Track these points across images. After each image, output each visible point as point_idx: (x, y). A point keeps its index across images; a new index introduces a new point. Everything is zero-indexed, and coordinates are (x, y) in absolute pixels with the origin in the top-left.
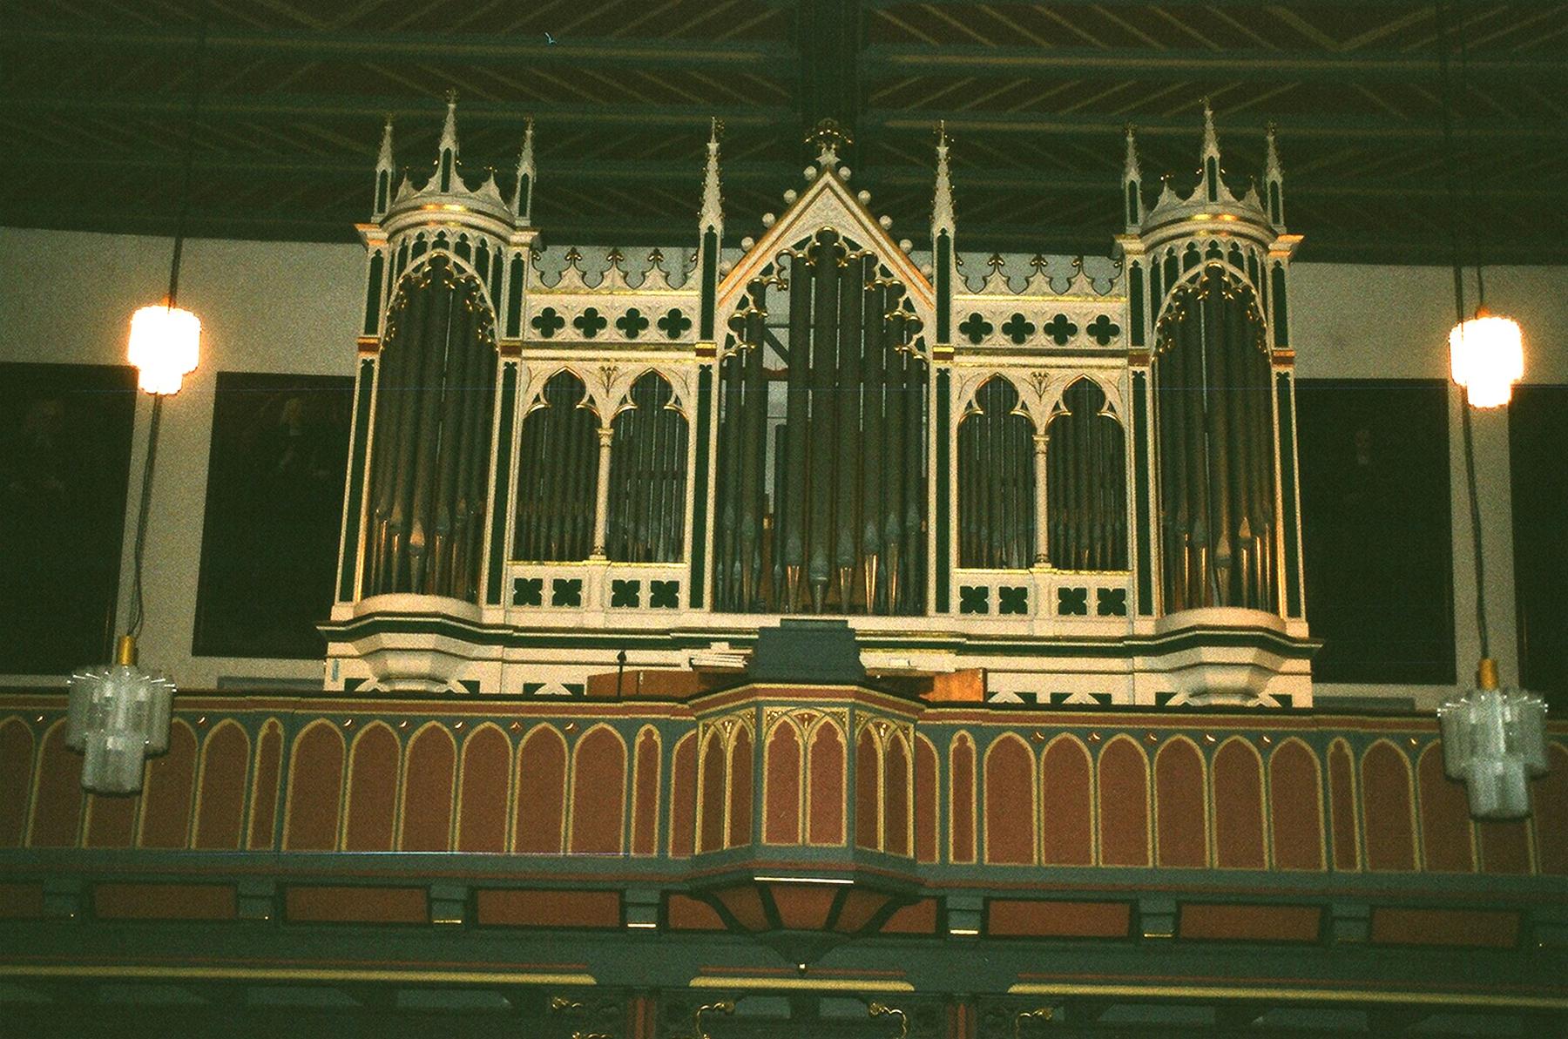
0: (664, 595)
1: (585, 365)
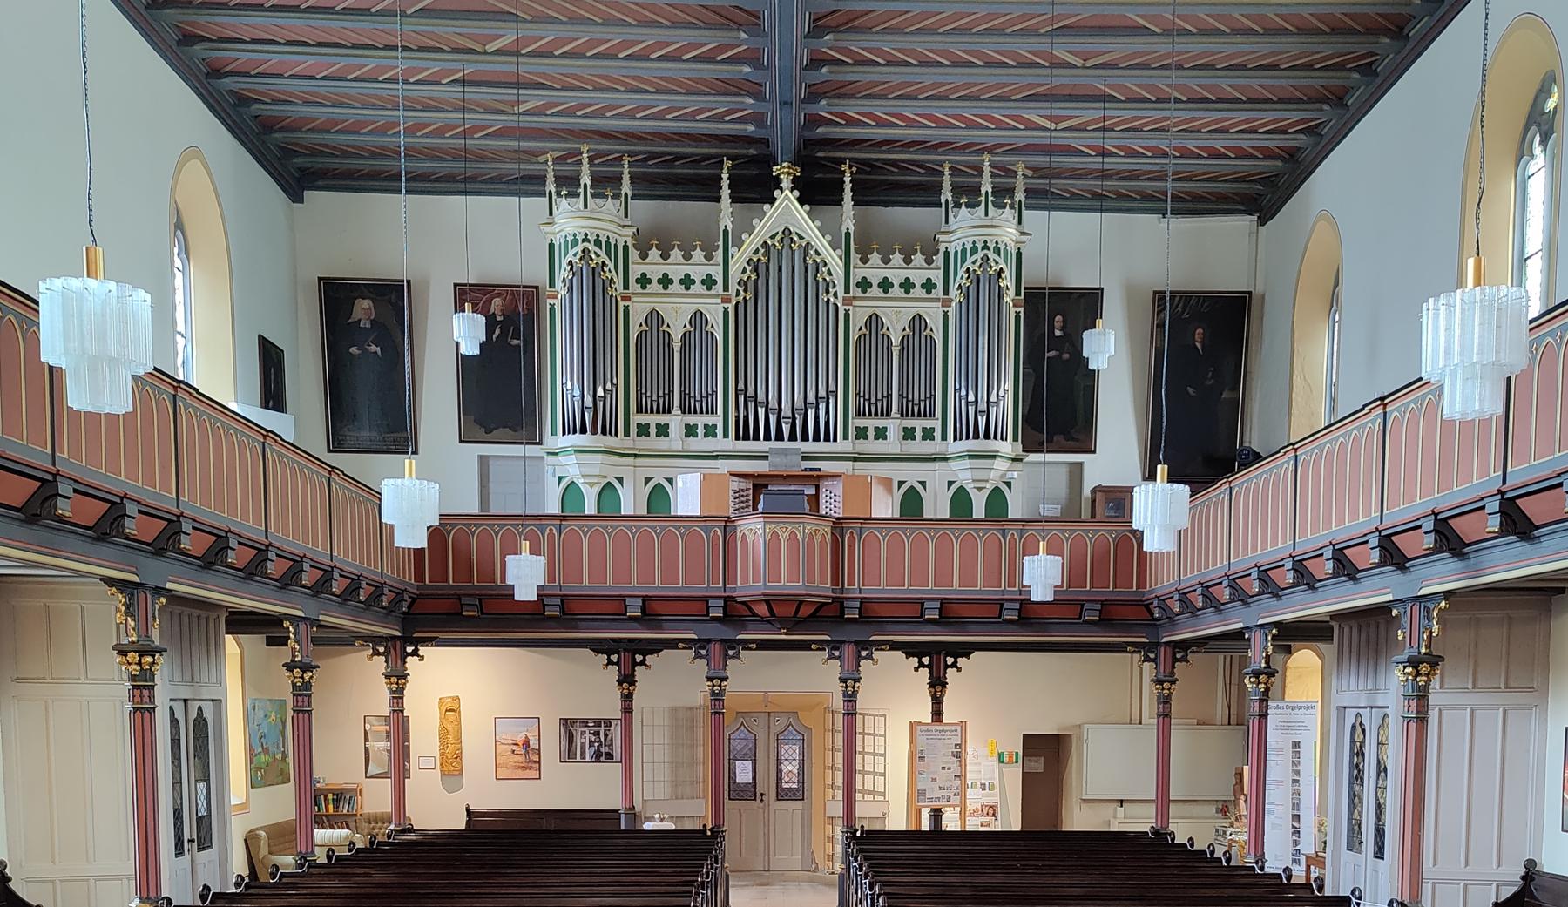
0: (710, 431)
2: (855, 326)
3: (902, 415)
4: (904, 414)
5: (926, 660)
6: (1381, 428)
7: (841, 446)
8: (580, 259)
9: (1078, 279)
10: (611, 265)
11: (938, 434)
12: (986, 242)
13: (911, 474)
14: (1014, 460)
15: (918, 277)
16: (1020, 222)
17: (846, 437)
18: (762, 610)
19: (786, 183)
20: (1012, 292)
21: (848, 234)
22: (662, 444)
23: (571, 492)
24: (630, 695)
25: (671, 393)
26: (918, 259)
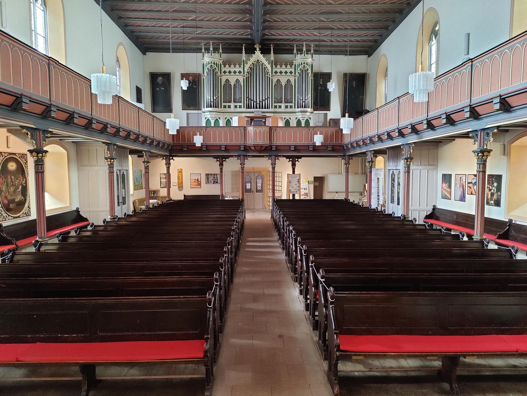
0: (240, 107)
2: (274, 83)
3: (285, 103)
4: (285, 102)
5: (291, 159)
6: (470, 70)
7: (271, 110)
8: (210, 67)
9: (326, 70)
10: (217, 69)
11: (293, 107)
12: (304, 62)
13: (287, 116)
14: (311, 113)
15: (288, 70)
16: (312, 57)
17: (272, 108)
18: (253, 148)
19: (258, 49)
20: (310, 74)
21: (272, 61)
23: (208, 121)
24: (222, 168)
25: (231, 98)
26: (289, 66)
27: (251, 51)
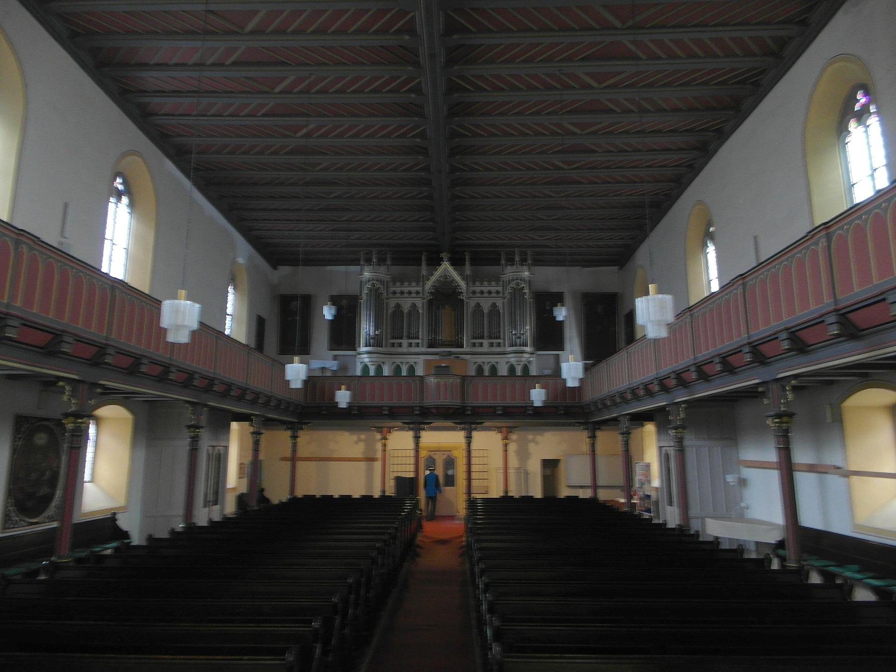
0: (417, 345)
1: (401, 301)
9: (554, 289)
13: (493, 359)
14: (531, 353)
22: (400, 350)
23: (366, 368)
27: (435, 262)
